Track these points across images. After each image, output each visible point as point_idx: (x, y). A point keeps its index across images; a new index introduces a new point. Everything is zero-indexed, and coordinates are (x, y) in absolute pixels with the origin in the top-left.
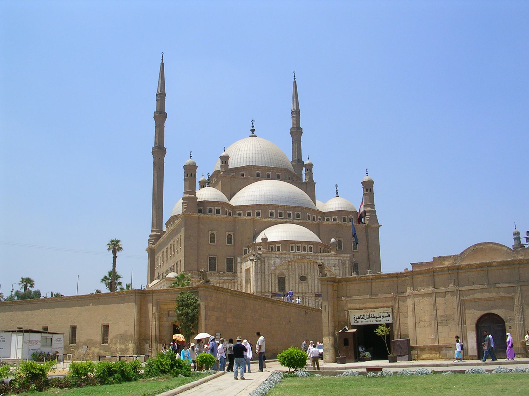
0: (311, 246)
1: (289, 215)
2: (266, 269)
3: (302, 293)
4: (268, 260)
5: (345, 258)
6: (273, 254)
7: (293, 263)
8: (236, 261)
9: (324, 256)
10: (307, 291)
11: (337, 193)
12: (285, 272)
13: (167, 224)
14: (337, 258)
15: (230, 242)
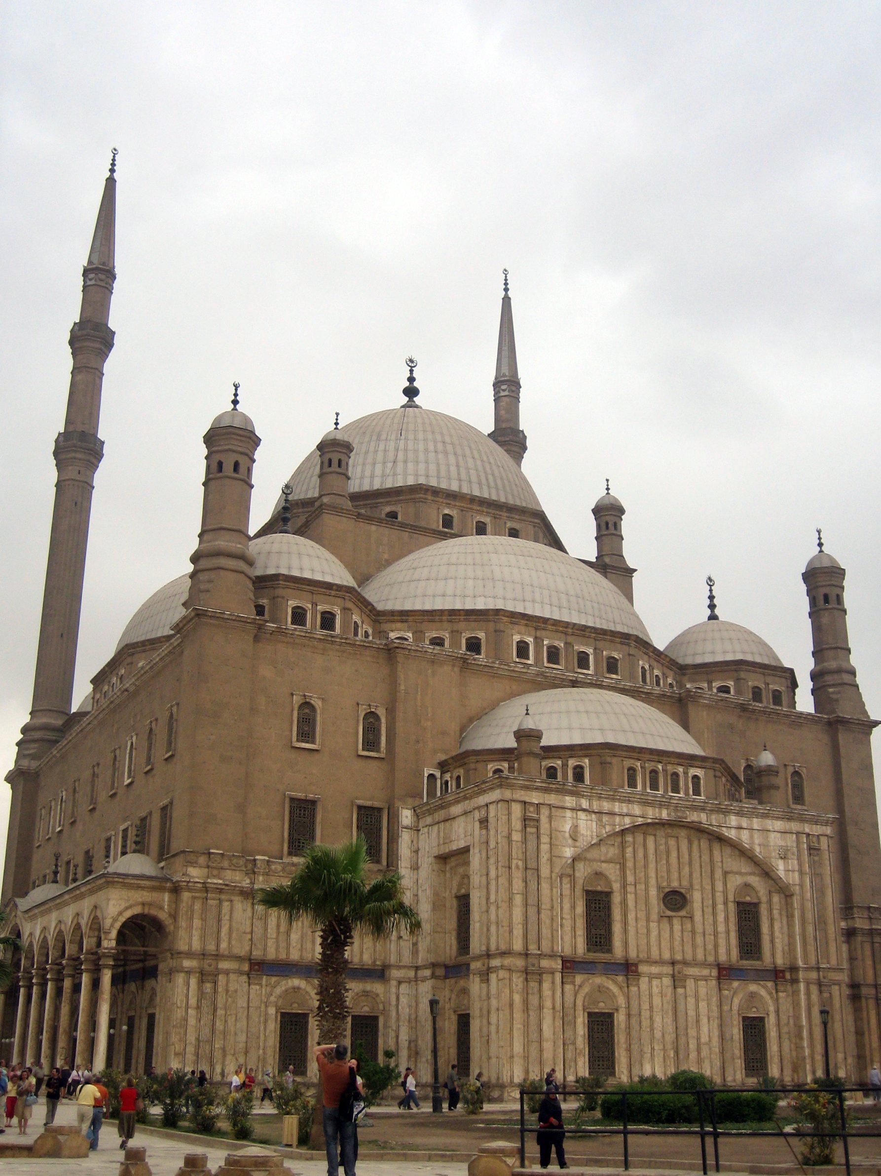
0: (699, 772)
1: (583, 661)
2: (544, 857)
3: (673, 963)
4: (550, 817)
5: (817, 830)
6: (573, 793)
7: (640, 838)
8: (394, 817)
9: (752, 814)
10: (689, 957)
11: (712, 607)
12: (611, 871)
13: (97, 681)
14: (794, 826)
15: (371, 743)
